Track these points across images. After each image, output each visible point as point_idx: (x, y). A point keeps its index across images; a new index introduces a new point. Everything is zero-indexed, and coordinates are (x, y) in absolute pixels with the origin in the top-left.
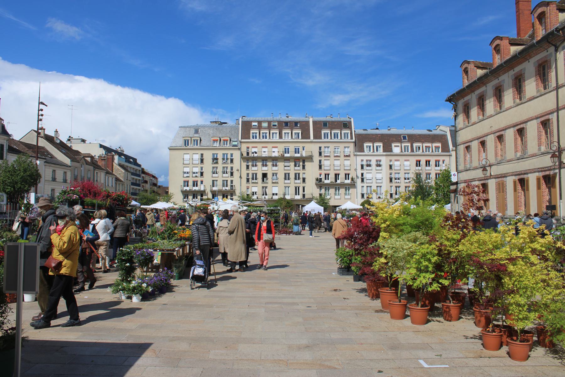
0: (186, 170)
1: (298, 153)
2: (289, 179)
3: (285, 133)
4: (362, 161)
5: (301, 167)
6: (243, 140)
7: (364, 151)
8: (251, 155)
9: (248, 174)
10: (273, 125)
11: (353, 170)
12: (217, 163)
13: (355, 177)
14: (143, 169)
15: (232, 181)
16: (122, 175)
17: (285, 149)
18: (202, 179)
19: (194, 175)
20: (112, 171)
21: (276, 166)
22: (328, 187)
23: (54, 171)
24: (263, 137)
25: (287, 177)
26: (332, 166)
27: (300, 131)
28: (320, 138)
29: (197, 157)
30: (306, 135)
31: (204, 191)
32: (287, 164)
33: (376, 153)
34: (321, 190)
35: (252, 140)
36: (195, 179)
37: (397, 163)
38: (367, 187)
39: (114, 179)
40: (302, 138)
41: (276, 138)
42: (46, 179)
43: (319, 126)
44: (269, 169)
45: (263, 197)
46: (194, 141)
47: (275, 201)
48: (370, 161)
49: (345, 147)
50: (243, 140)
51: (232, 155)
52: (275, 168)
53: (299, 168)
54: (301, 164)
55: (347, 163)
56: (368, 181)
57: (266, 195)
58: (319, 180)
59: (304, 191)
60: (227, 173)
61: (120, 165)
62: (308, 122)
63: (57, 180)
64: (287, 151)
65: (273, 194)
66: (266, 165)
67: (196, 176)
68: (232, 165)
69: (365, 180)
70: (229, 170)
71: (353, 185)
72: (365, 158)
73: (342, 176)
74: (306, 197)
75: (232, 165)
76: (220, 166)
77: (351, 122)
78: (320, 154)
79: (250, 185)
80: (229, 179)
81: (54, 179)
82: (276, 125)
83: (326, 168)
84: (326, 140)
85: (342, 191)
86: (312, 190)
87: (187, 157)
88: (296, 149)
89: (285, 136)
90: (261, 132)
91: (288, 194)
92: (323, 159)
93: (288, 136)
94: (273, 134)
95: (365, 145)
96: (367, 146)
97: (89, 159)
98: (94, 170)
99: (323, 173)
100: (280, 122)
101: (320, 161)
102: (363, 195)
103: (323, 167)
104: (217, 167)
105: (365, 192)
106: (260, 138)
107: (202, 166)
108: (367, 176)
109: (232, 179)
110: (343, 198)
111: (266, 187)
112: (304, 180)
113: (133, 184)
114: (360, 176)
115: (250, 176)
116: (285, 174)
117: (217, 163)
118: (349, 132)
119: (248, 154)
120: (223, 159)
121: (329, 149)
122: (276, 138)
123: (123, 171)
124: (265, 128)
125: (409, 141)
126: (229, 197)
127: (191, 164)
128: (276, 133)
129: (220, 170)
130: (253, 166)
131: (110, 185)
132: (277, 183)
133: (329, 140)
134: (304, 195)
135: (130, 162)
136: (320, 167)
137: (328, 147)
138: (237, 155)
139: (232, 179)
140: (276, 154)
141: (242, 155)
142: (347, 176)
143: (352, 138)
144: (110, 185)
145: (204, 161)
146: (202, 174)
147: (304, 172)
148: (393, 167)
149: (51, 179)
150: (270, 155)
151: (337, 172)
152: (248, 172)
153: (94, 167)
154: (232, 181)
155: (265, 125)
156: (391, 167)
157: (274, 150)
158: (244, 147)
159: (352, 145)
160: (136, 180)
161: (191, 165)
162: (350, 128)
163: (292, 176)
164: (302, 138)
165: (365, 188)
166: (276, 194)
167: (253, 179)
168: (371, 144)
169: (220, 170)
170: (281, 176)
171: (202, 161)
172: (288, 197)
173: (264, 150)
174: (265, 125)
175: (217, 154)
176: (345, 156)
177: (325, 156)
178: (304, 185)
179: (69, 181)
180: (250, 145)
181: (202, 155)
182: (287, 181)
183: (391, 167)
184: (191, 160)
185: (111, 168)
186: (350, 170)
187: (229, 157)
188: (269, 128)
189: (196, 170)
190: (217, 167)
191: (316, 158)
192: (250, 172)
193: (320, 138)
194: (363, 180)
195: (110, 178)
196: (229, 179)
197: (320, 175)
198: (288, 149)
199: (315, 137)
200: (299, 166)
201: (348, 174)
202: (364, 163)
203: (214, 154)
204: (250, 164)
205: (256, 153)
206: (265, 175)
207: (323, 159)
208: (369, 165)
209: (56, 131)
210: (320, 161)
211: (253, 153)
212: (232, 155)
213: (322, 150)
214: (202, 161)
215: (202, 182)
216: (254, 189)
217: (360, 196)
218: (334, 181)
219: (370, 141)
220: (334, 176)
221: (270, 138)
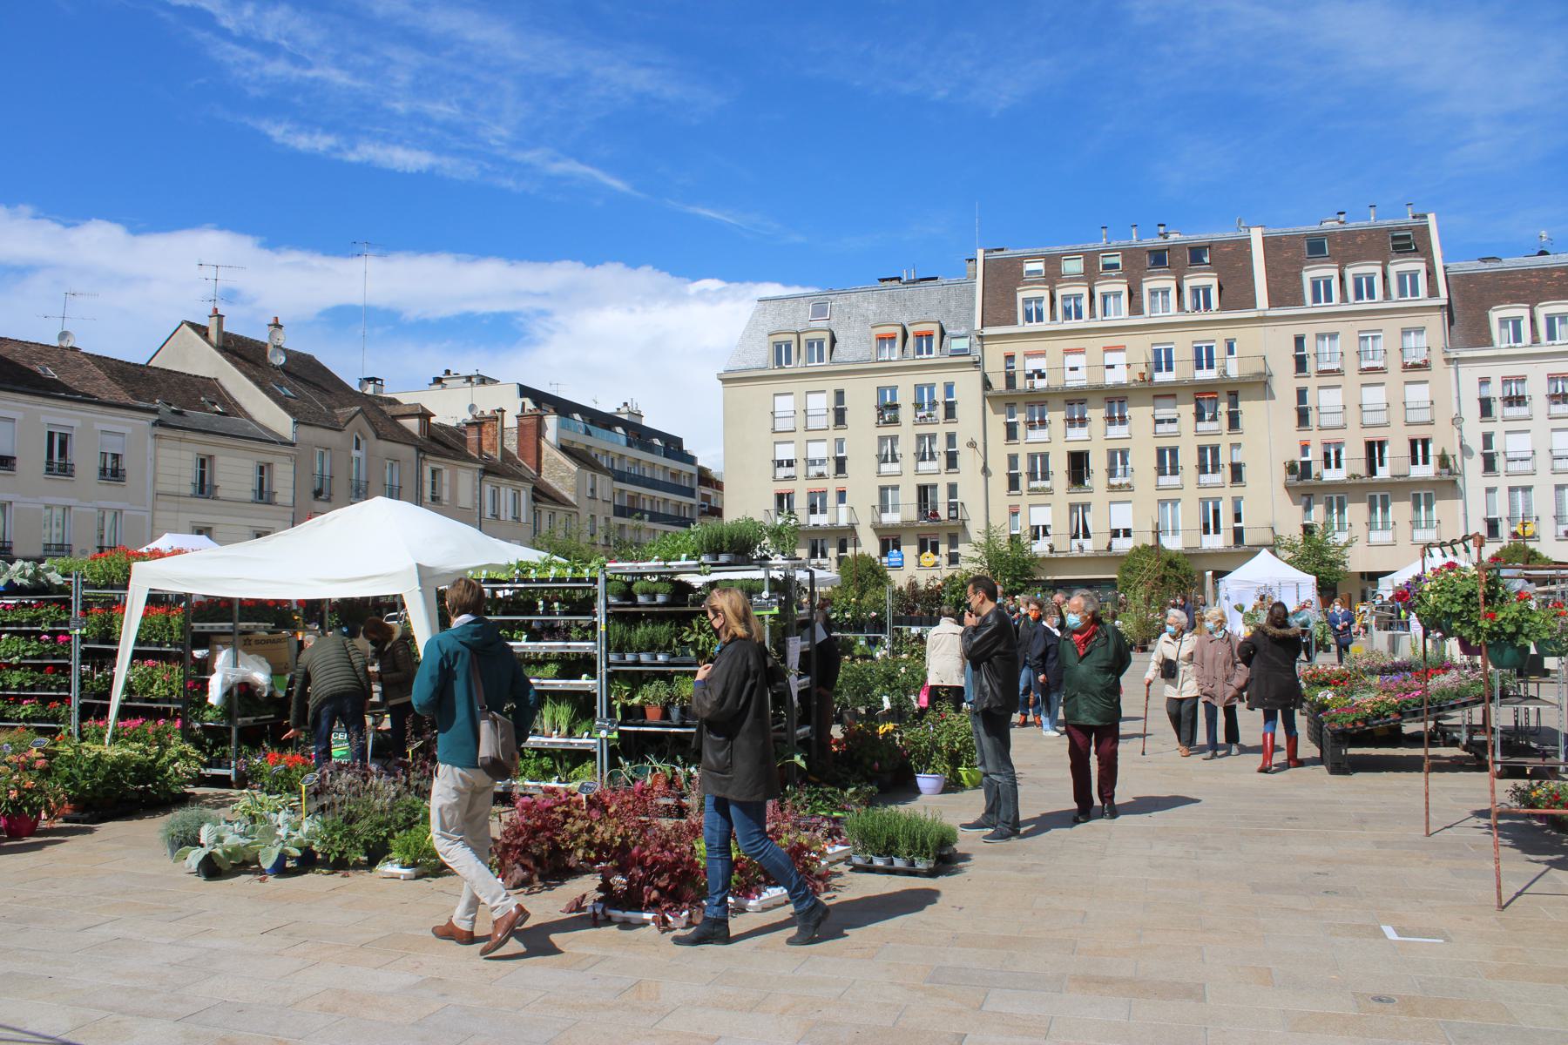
0: (785, 453)
1: (1210, 366)
2: (1175, 472)
3: (1153, 293)
4: (1484, 382)
5: (1224, 420)
6: (988, 331)
7: (1489, 343)
8: (1021, 383)
10: (1106, 267)
11: (1443, 423)
12: (895, 421)
13: (1453, 449)
14: (702, 470)
15: (953, 489)
16: (570, 482)
17: (1157, 353)
18: (841, 483)
19: (813, 471)
20: (539, 470)
21: (1123, 420)
22: (1337, 497)
24: (1067, 312)
25: (1166, 461)
26: (1353, 412)
27: (1212, 281)
28: (1298, 300)
29: (821, 403)
30: (1236, 293)
31: (852, 529)
32: (1164, 413)
33: (1545, 346)
34: (1308, 508)
35: (1023, 327)
36: (818, 485)
38: (1512, 489)
39: (525, 496)
40: (1223, 307)
41: (1120, 313)
42: (160, 488)
43: (1291, 255)
44: (1095, 436)
45: (1075, 542)
46: (811, 345)
47: (1119, 558)
49: (1405, 332)
50: (988, 331)
51: (949, 388)
52: (1117, 431)
53: (1213, 426)
54: (1223, 407)
55: (1418, 394)
56: (1513, 467)
57: (1087, 535)
58: (1299, 471)
59: (1238, 518)
60: (932, 457)
61: (565, 449)
62: (1246, 244)
64: (1162, 360)
65: (1115, 534)
66: (1083, 422)
67: (821, 475)
68: (950, 428)
69: (1500, 463)
70: (940, 446)
71: (1448, 485)
72: (1496, 372)
73: (1396, 451)
75: (950, 428)
76: (907, 432)
77: (1426, 227)
78: (1301, 364)
79: (1023, 500)
80: (942, 482)
81: (204, 487)
82: (1116, 266)
83: (1327, 421)
84: (1323, 307)
85: (1400, 510)
86: (1270, 507)
87: (785, 405)
88: (1198, 351)
89: (1152, 303)
90: (1059, 294)
91: (1175, 532)
92: (1311, 383)
93: (1166, 303)
94: (1105, 297)
95: (1495, 316)
97: (413, 425)
98: (420, 462)
99: (1316, 439)
100: (1130, 254)
101: (1301, 394)
103: (1313, 416)
104: (894, 439)
105: (1501, 511)
106: (1053, 317)
107: (840, 434)
108: (1509, 444)
109: (952, 479)
110: (1404, 542)
111: (1086, 507)
112: (1237, 472)
113: (620, 511)
114: (1477, 445)
115: (1023, 467)
116: (1161, 452)
117: (895, 421)
118: (1420, 266)
119: (1010, 379)
120: (918, 406)
121: (1338, 345)
123: (574, 468)
124: (1074, 279)
126: (943, 548)
127: (800, 429)
128: (1118, 295)
129: (907, 447)
130: (1031, 425)
131: (506, 513)
132: (1129, 487)
133: (1336, 304)
134: (1238, 535)
135: (650, 448)
136: (1303, 417)
137: (1333, 336)
138: (967, 389)
139: (952, 479)
140: (1118, 376)
141: (987, 384)
142: (1418, 448)
143: (1433, 292)
144: (506, 513)
145: (848, 416)
146: (840, 465)
147: (1235, 439)
149: (190, 490)
150: (1096, 381)
151: (1375, 435)
152: (1013, 449)
153: (419, 450)
154: (953, 489)
157: (1110, 358)
158: (994, 357)
159: (1437, 322)
160: (678, 505)
161: (801, 436)
162: (1428, 255)
163: (1188, 459)
164: (1223, 307)
165: (1501, 497)
166: (1127, 533)
167: (1032, 476)
169: (907, 447)
170: (1143, 461)
171: (840, 417)
172: (1172, 543)
173: (1072, 360)
174: (1073, 266)
175: (894, 389)
176: (1407, 367)
177: (1322, 373)
178: (1237, 491)
179: (523, 519)
180: (1017, 348)
181: (840, 395)
182: (1166, 480)
184: (801, 415)
185: (533, 459)
187: (939, 395)
188: (1090, 275)
189: (820, 451)
190: (894, 439)
191: (1285, 383)
192: (1022, 450)
193: (1298, 300)
194: (1489, 464)
195: (506, 494)
196: (942, 482)
197: (1305, 448)
198: (1169, 352)
199: (1275, 301)
200: (1214, 419)
201: (1425, 443)
202: (1495, 391)
203: (881, 391)
204: (1020, 418)
205: (1042, 376)
206: (1078, 464)
207: (1311, 383)
208: (1516, 400)
210: (1301, 394)
211: (1030, 376)
212: (949, 388)
213: (1309, 348)
214: (840, 417)
215: (842, 496)
216: (1040, 517)
218: (1361, 469)
219: (1515, 299)
220: (1362, 452)
221: (1092, 315)
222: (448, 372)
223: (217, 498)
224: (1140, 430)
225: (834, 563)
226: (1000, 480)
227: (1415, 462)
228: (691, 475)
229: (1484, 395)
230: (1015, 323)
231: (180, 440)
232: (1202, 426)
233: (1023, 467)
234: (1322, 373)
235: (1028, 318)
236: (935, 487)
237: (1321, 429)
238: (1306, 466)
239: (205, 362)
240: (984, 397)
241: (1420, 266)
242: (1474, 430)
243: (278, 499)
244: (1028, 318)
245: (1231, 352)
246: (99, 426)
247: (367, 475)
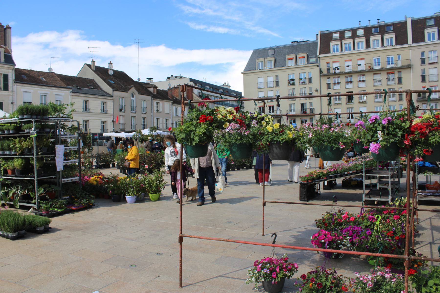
3: (374, 41)
5: (397, 80)
6: (321, 56)
8: (332, 71)
12: (293, 84)
23: (86, 102)
24: (346, 49)
27: (393, 36)
29: (271, 79)
30: (401, 39)
40: (397, 44)
45: (348, 120)
53: (393, 82)
63: (91, 111)
75: (310, 85)
78: (423, 61)
87: (261, 80)
89: (374, 44)
90: (343, 43)
93: (378, 44)
97: (151, 90)
103: (427, 78)
106: (342, 50)
107: (277, 88)
117: (293, 84)
119: (328, 70)
122: (362, 48)
127: (266, 87)
128: (362, 42)
136: (423, 78)
138: (315, 73)
141: (321, 72)
150: (355, 70)
155: (348, 34)
157: (360, 62)
164: (397, 44)
171: (277, 83)
173: (347, 63)
180: (330, 60)
181: (277, 76)
184: (266, 83)
193: (423, 40)
195: (180, 108)
199: (414, 41)
205: (338, 69)
207: (426, 67)
209: (111, 63)
213: (426, 56)
214: (277, 83)
221: (354, 49)
222: (172, 76)
223: (108, 113)
224: (369, 83)
230: (330, 53)
231: (78, 96)
232: (389, 83)
236: (306, 103)
237: (429, 82)
239: (91, 75)
240: (320, 76)
243: (108, 112)
244: (334, 51)
245: (399, 58)
246: (55, 93)
247: (136, 104)
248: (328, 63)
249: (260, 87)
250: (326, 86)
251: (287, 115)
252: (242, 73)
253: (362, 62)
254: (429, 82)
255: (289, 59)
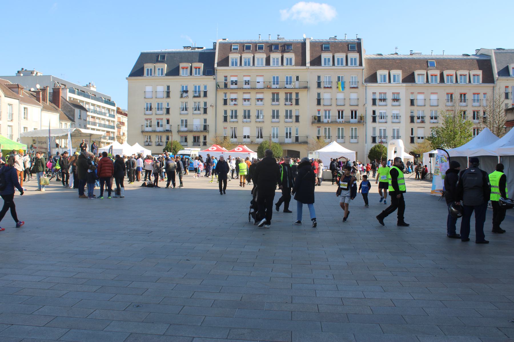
4: (374, 93)
5: (294, 102)
9: (226, 112)
11: (361, 105)
14: (118, 109)
25: (275, 115)
29: (161, 89)
37: (420, 97)
46: (159, 69)
48: (385, 93)
55: (354, 96)
60: (199, 110)
74: (300, 140)
78: (319, 85)
89: (274, 62)
93: (278, 62)
96: (381, 75)
101: (319, 94)
102: (374, 139)
103: (322, 101)
105: (377, 134)
106: (241, 64)
115: (229, 114)
116: (273, 111)
125: (437, 68)
127: (154, 97)
136: (319, 103)
148: (415, 102)
156: (412, 102)
163: (282, 114)
168: (386, 72)
177: (325, 88)
181: (168, 87)
183: (412, 102)
186: (357, 105)
187: (202, 89)
197: (319, 111)
202: (378, 97)
210: (319, 94)
217: (370, 140)
219: (385, 68)
222: (22, 69)
225: (165, 144)
226: (221, 118)
227: (352, 118)
228: (113, 110)
229: (374, 98)
233: (229, 114)
234: (325, 88)
235: (233, 65)
237: (324, 105)
238: (319, 117)
241: (357, 55)
242: (370, 108)
244: (233, 65)
248: (226, 77)
249: (147, 96)
250: (222, 102)
251: (179, 132)
252: (127, 78)
253: (259, 79)
254: (324, 105)
255: (183, 68)
